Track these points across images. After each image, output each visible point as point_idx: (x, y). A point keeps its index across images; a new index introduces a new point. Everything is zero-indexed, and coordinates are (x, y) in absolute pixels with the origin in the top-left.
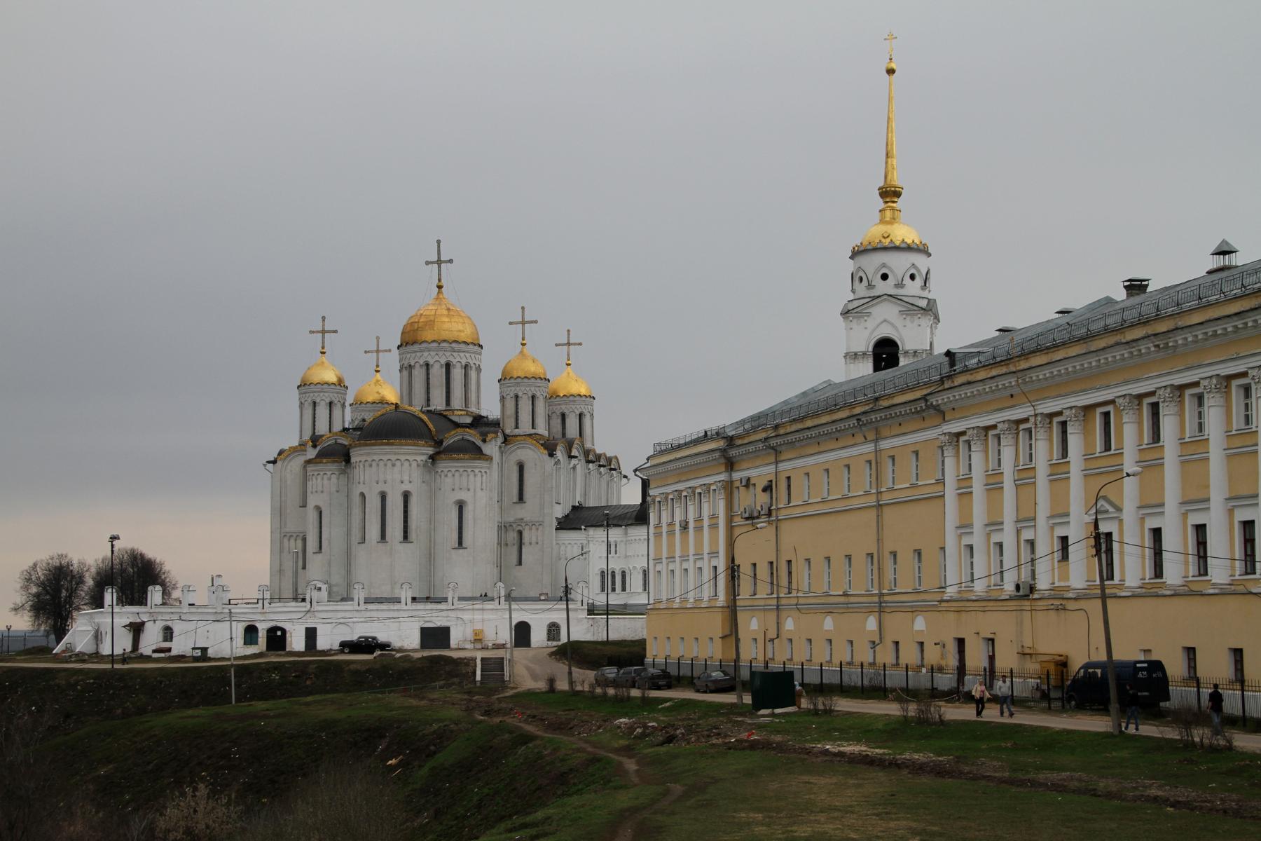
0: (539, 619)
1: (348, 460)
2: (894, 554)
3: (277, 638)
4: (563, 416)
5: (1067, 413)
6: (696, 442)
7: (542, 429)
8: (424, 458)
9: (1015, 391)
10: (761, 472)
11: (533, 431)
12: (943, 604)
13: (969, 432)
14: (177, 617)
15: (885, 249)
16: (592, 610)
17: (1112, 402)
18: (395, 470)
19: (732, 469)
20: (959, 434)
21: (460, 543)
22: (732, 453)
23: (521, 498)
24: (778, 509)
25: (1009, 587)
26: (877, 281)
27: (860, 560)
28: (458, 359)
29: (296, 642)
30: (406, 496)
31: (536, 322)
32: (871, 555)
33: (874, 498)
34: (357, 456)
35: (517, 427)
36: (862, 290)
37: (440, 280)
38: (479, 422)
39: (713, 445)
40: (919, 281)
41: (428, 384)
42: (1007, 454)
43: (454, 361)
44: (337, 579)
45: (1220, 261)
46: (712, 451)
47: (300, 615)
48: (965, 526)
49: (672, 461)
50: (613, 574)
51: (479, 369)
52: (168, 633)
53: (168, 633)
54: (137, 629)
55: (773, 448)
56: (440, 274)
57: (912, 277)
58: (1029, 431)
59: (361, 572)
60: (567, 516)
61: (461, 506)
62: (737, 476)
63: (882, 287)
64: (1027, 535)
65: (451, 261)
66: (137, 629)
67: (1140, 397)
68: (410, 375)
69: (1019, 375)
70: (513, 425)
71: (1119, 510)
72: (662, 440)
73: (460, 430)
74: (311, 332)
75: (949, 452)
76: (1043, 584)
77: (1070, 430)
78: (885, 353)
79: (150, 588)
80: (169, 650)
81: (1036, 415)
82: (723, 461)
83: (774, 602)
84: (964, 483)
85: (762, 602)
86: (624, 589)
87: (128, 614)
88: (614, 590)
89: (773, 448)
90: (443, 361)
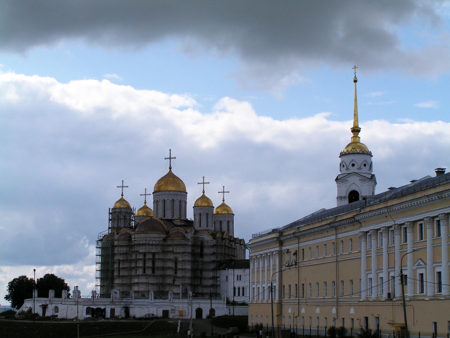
2: (343, 282)
4: (221, 222)
5: (406, 224)
6: (269, 234)
7: (210, 228)
8: (161, 239)
9: (387, 214)
10: (292, 246)
11: (207, 228)
12: (361, 303)
13: (370, 232)
14: (60, 302)
15: (353, 153)
16: (228, 303)
19: (282, 245)
22: (282, 239)
24: (299, 262)
25: (385, 296)
26: (351, 167)
27: (330, 284)
29: (108, 315)
31: (209, 183)
32: (334, 282)
33: (335, 258)
35: (200, 227)
36: (344, 170)
37: (170, 166)
39: (274, 235)
40: (368, 167)
41: (165, 208)
42: (385, 240)
43: (175, 199)
46: (274, 238)
47: (108, 303)
48: (368, 269)
49: (260, 241)
50: (239, 288)
51: (186, 203)
52: (56, 309)
54: (44, 307)
55: (297, 237)
56: (170, 163)
57: (365, 165)
58: (393, 231)
62: (284, 248)
63: (352, 170)
65: (175, 158)
66: (44, 307)
67: (433, 218)
68: (157, 204)
69: (389, 208)
70: (199, 225)
71: (426, 264)
72: (255, 233)
73: (176, 228)
74: (118, 187)
75: (363, 239)
78: (353, 196)
79: (50, 291)
80: (57, 316)
81: (395, 225)
82: (278, 242)
83: (297, 301)
84: (368, 252)
85: (292, 301)
86: (243, 295)
87: (43, 301)
88: (239, 295)
89: (297, 237)
90: (171, 199)
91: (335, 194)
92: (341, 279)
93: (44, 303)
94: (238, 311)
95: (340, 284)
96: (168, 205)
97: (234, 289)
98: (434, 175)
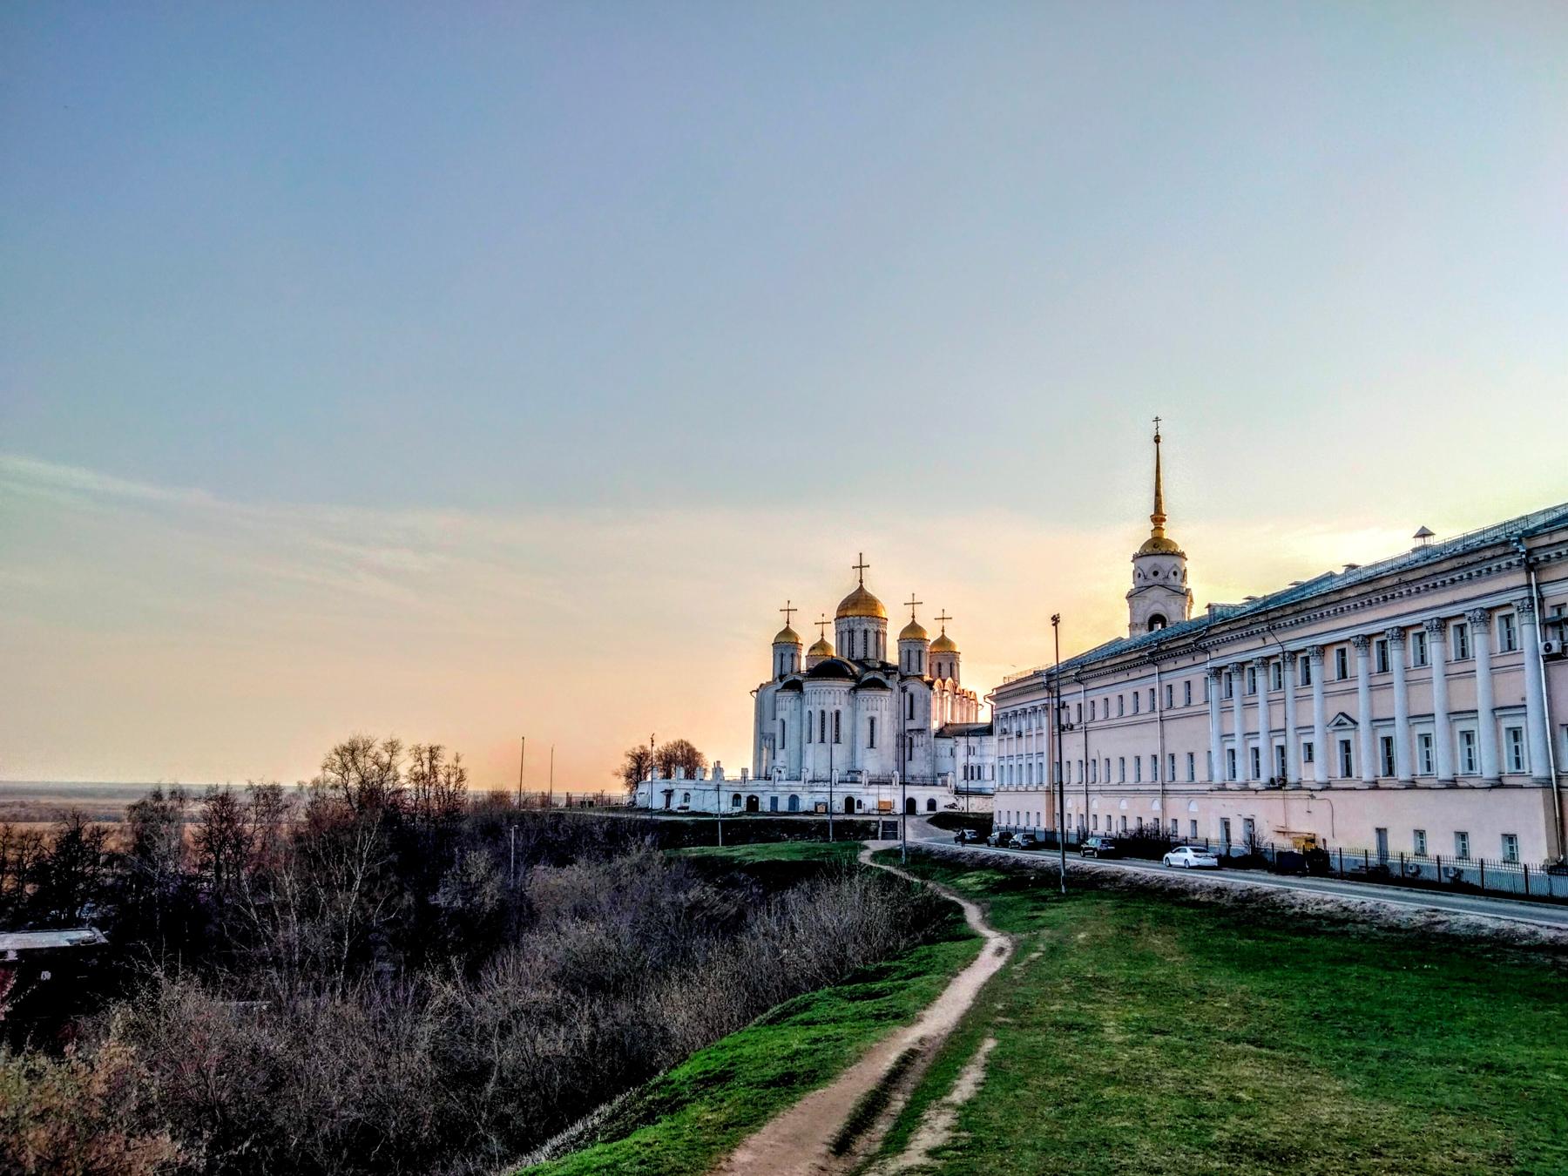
0: (921, 796)
1: (801, 690)
3: (753, 803)
6: (1030, 678)
10: (1073, 697)
17: (1348, 641)
18: (831, 696)
20: (1220, 669)
21: (872, 745)
23: (911, 717)
25: (1264, 778)
28: (872, 627)
30: (838, 713)
34: (807, 686)
36: (1142, 582)
38: (885, 665)
44: (794, 765)
45: (1420, 542)
53: (687, 796)
54: (669, 794)
58: (1278, 664)
59: (809, 762)
60: (941, 730)
61: (872, 721)
63: (1155, 580)
64: (1279, 741)
66: (669, 794)
76: (1292, 779)
77: (1312, 662)
91: (1126, 618)
92: (1168, 751)
93: (668, 787)
94: (976, 805)
95: (1167, 758)
96: (859, 637)
97: (966, 768)
98: (1340, 571)
